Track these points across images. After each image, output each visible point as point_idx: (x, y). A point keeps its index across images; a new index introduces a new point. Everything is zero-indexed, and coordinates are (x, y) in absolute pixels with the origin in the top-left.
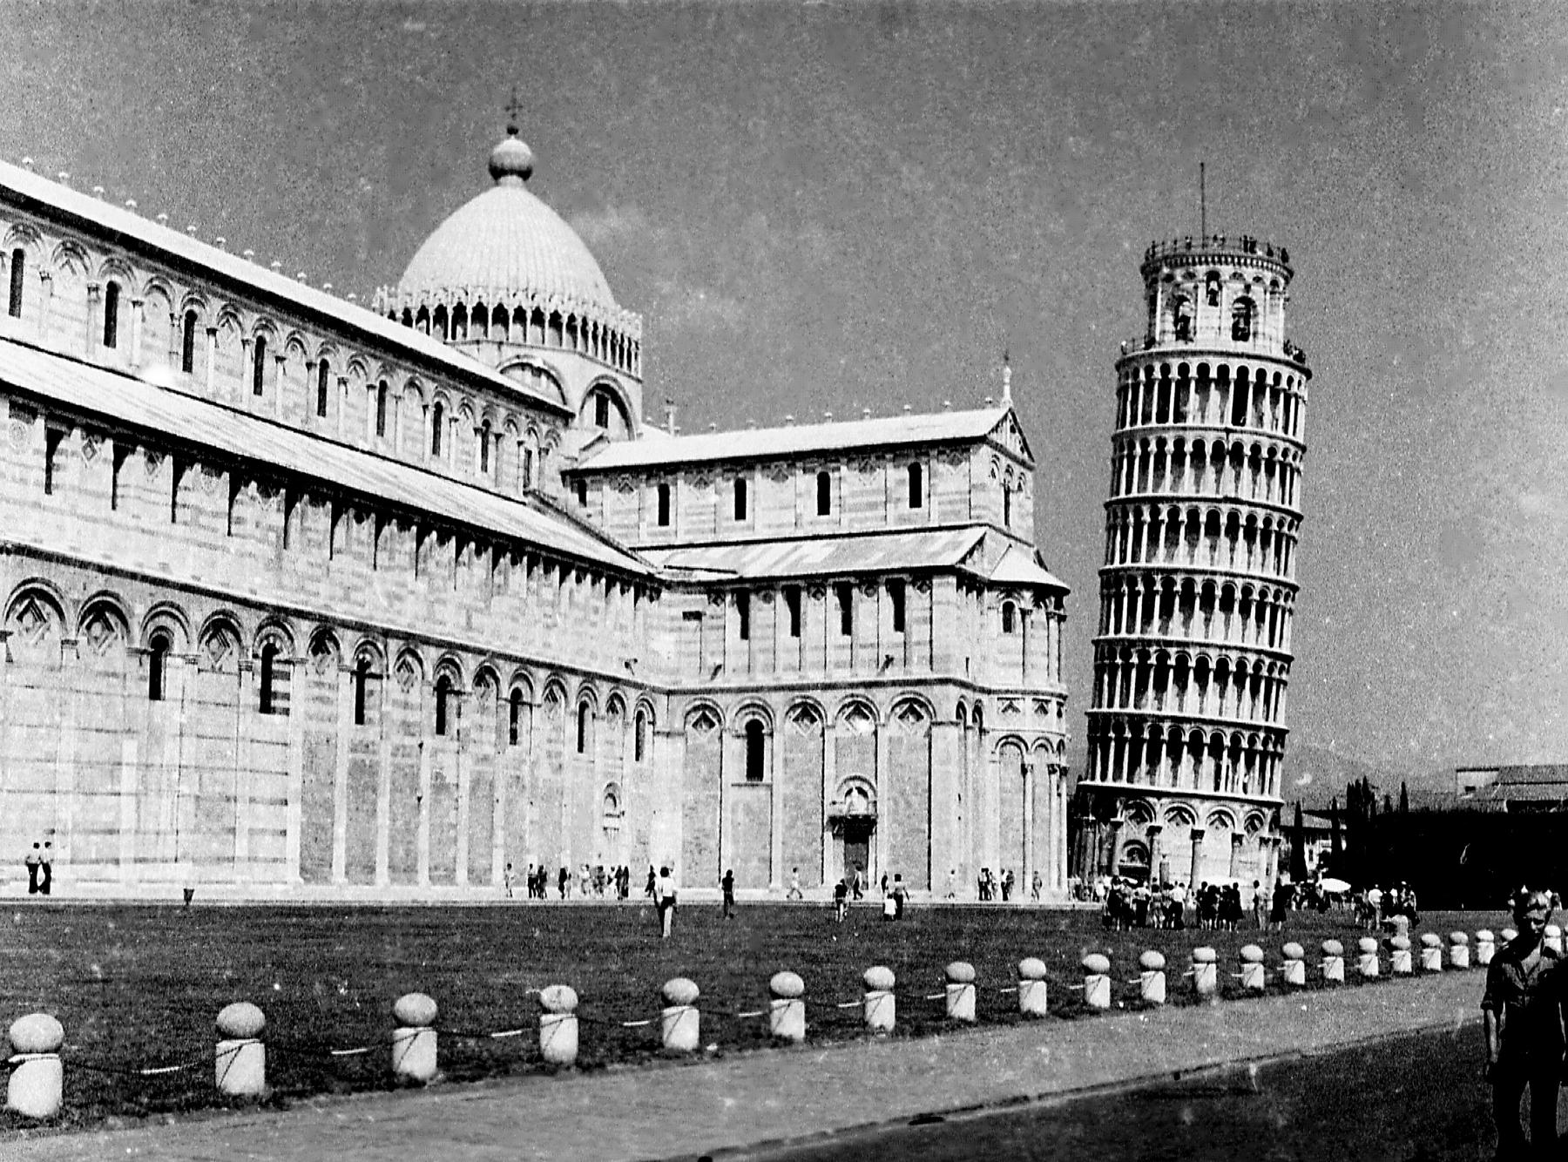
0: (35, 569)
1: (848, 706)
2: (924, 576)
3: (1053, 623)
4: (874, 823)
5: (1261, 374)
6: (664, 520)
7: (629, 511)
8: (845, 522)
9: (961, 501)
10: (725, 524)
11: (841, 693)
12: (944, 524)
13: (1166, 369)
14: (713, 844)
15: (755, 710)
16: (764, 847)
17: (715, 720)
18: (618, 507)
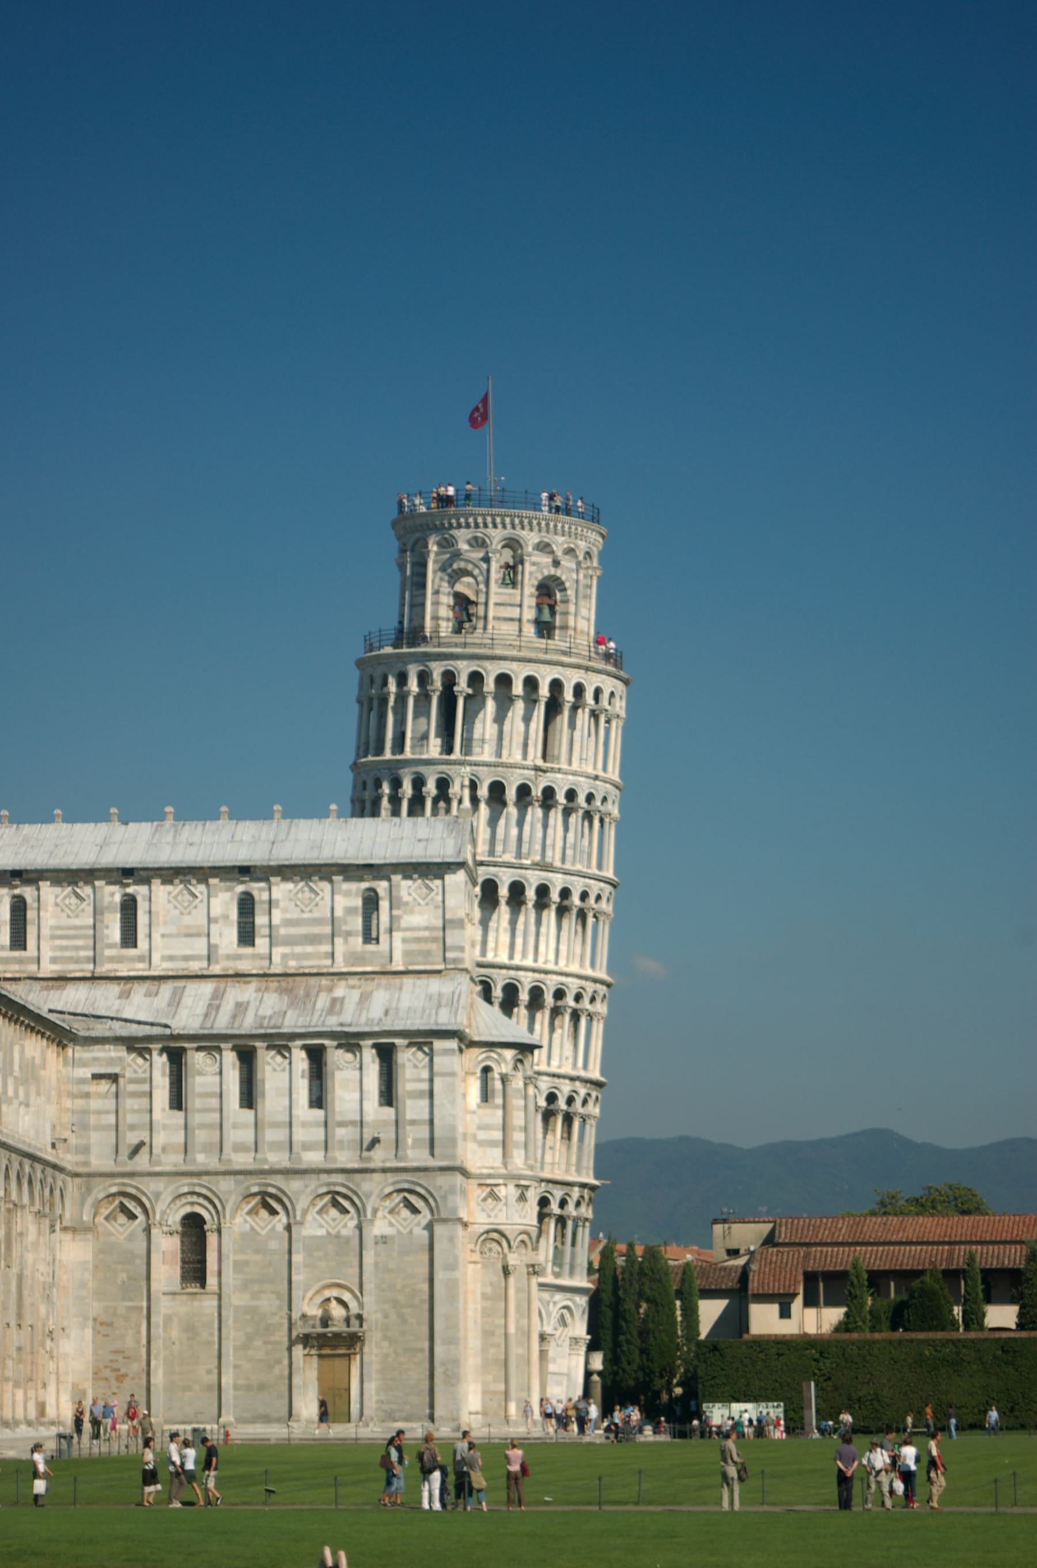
8: (276, 959)
9: (434, 940)
10: (108, 952)
12: (411, 968)
13: (449, 679)
14: (137, 1367)
15: (195, 1199)
16: (209, 1372)
17: (137, 1211)
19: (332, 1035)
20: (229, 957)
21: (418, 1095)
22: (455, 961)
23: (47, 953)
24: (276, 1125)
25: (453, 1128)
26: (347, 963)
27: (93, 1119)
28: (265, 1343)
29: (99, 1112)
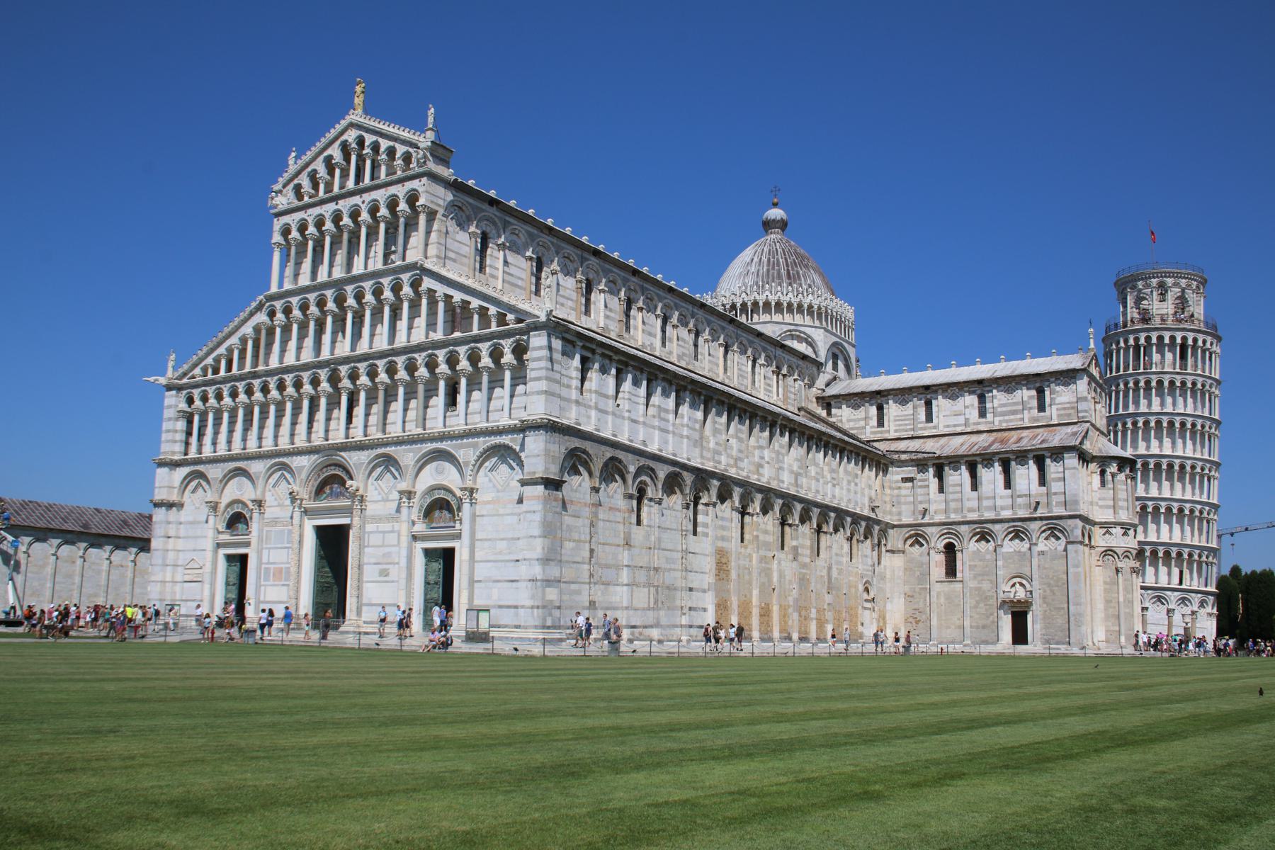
0: (576, 443)
1: (1010, 533)
2: (1058, 453)
3: (1129, 481)
4: (1031, 603)
5: (1195, 340)
6: (880, 423)
7: (859, 420)
8: (996, 423)
9: (1073, 408)
10: (920, 426)
11: (1006, 525)
13: (1137, 339)
16: (959, 619)
17: (924, 542)
18: (854, 417)
19: (1012, 452)
20: (975, 424)
21: (1059, 479)
22: (1083, 417)
23: (892, 428)
24: (988, 498)
25: (1075, 495)
26: (1029, 421)
27: (903, 500)
28: (985, 605)
29: (905, 496)
